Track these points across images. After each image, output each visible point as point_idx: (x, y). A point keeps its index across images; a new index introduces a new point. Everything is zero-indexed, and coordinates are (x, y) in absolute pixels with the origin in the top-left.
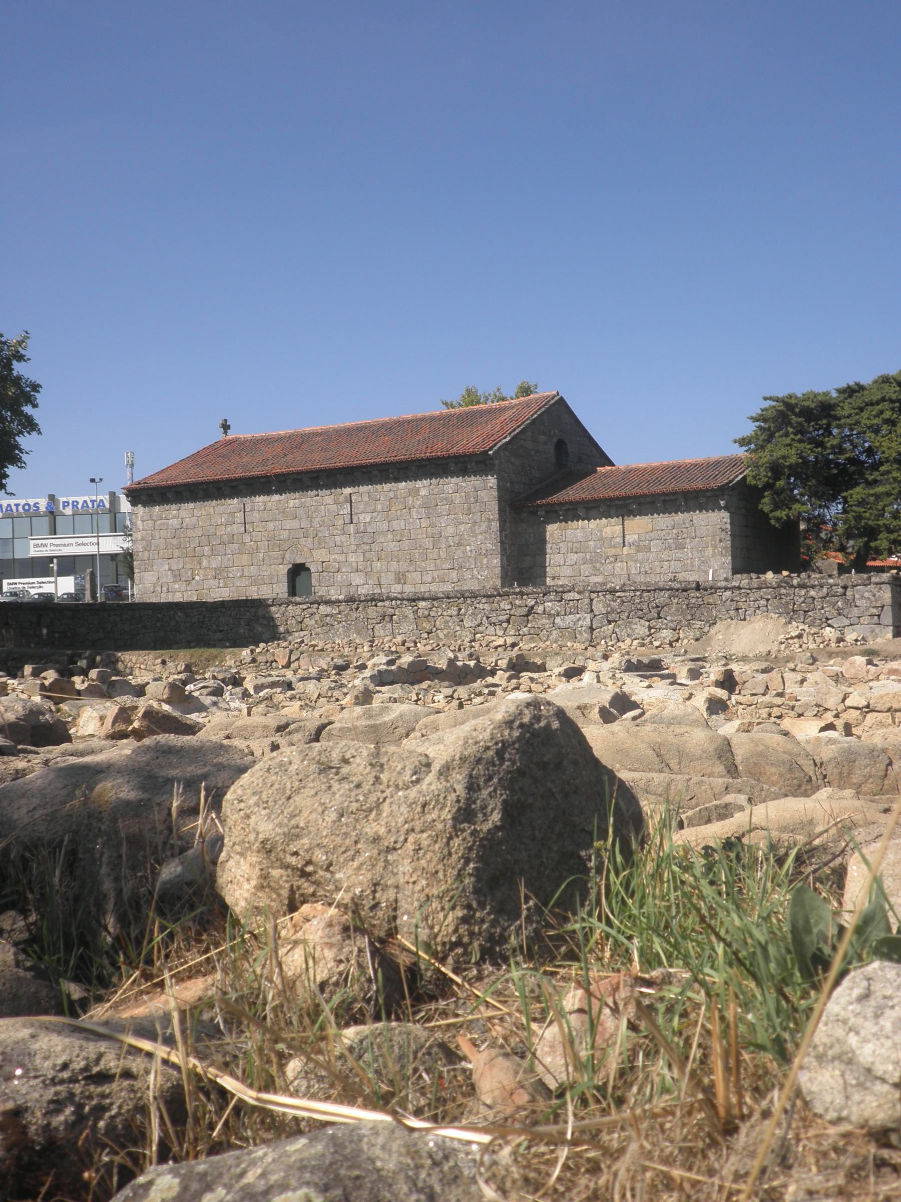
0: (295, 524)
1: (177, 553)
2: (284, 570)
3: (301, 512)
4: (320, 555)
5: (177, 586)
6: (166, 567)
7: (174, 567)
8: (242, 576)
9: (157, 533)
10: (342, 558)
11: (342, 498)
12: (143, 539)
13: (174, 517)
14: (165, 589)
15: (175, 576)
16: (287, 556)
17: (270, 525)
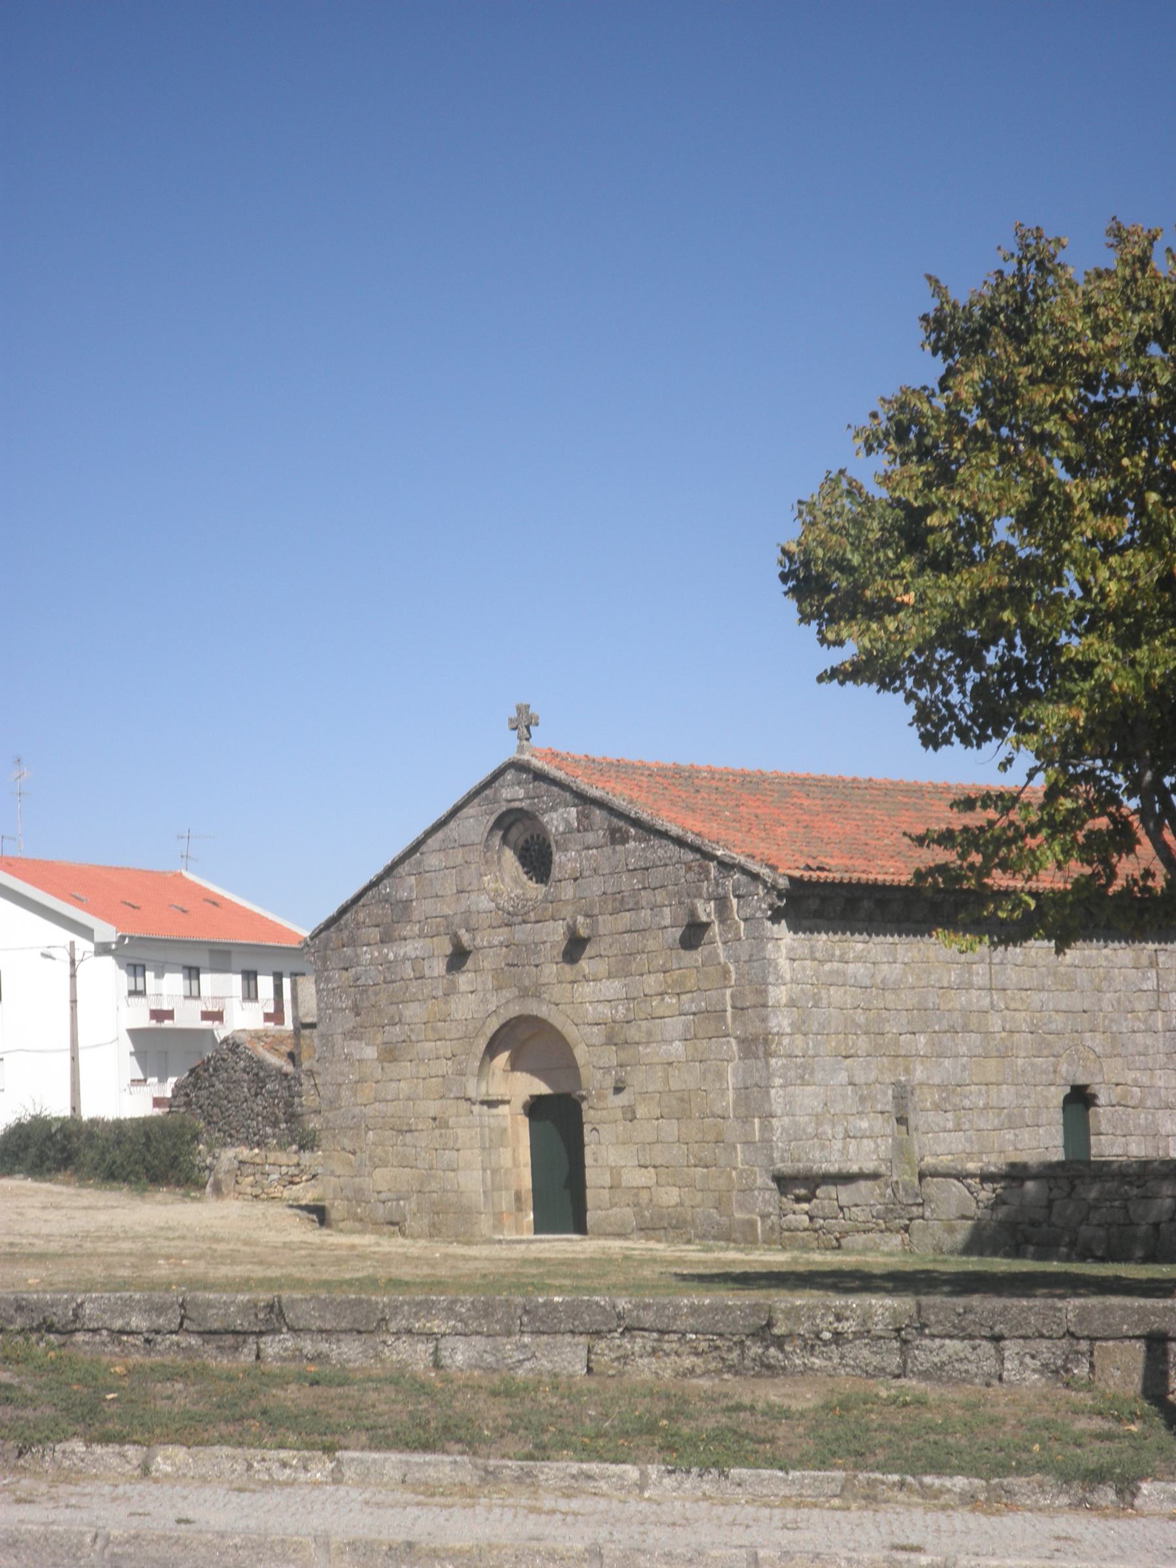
0: (1076, 1001)
1: (863, 1044)
2: (1058, 1094)
3: (1082, 976)
4: (1113, 1069)
5: (864, 1124)
6: (843, 1077)
7: (860, 1079)
8: (987, 1107)
9: (823, 993)
10: (1145, 1079)
11: (1144, 961)
12: (792, 1003)
13: (858, 959)
14: (840, 1130)
15: (862, 1099)
16: (1064, 1068)
17: (1036, 998)
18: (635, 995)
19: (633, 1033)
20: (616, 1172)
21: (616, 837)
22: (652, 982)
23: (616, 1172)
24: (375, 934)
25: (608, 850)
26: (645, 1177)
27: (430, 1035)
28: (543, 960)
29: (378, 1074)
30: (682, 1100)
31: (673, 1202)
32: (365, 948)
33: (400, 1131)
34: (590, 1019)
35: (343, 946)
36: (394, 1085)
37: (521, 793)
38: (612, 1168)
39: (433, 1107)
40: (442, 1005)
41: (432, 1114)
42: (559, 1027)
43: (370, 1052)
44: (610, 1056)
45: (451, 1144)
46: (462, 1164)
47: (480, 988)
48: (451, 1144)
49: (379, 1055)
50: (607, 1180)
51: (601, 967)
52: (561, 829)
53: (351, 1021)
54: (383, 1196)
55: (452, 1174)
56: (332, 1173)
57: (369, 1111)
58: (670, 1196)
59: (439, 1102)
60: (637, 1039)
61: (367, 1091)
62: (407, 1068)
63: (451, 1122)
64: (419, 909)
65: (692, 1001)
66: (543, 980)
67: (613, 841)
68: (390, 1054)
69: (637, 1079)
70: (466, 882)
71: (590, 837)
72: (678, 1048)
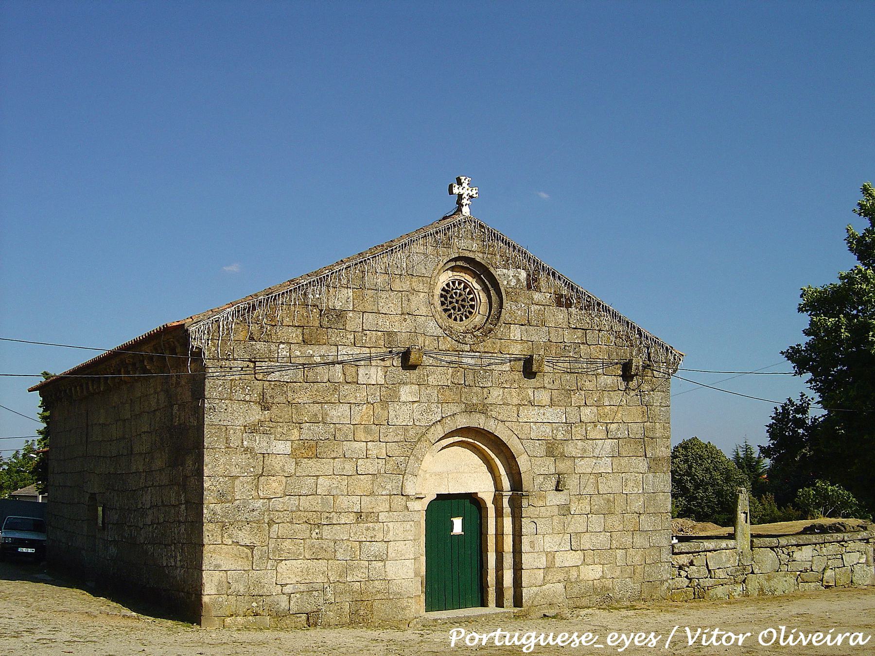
18: (573, 421)
19: (571, 449)
20: (551, 556)
21: (561, 301)
22: (587, 413)
23: (551, 556)
24: (295, 335)
25: (554, 308)
26: (574, 558)
27: (361, 435)
28: (490, 384)
29: (291, 467)
30: (609, 501)
31: (598, 576)
32: (282, 346)
33: (319, 525)
34: (533, 436)
35: (252, 339)
36: (312, 480)
37: (475, 247)
38: (547, 553)
39: (354, 503)
40: (378, 410)
41: (357, 508)
42: (504, 439)
43: (282, 447)
44: (549, 466)
45: (380, 536)
46: (392, 554)
47: (423, 399)
48: (380, 536)
49: (294, 450)
50: (543, 562)
51: (544, 397)
52: (513, 284)
53: (256, 414)
54: (288, 589)
55: (381, 564)
56: (217, 567)
57: (277, 504)
58: (592, 573)
59: (368, 499)
60: (574, 454)
61: (275, 485)
62: (325, 466)
63: (382, 517)
64: (353, 322)
65: (618, 429)
66: (489, 401)
67: (559, 304)
68: (310, 449)
69: (572, 483)
70: (413, 306)
71: (537, 296)
72: (605, 465)
